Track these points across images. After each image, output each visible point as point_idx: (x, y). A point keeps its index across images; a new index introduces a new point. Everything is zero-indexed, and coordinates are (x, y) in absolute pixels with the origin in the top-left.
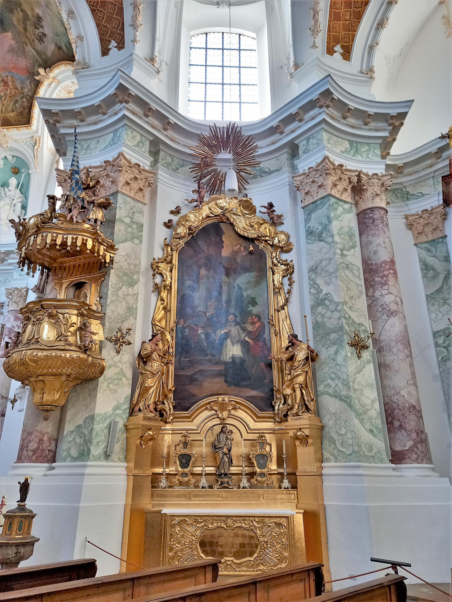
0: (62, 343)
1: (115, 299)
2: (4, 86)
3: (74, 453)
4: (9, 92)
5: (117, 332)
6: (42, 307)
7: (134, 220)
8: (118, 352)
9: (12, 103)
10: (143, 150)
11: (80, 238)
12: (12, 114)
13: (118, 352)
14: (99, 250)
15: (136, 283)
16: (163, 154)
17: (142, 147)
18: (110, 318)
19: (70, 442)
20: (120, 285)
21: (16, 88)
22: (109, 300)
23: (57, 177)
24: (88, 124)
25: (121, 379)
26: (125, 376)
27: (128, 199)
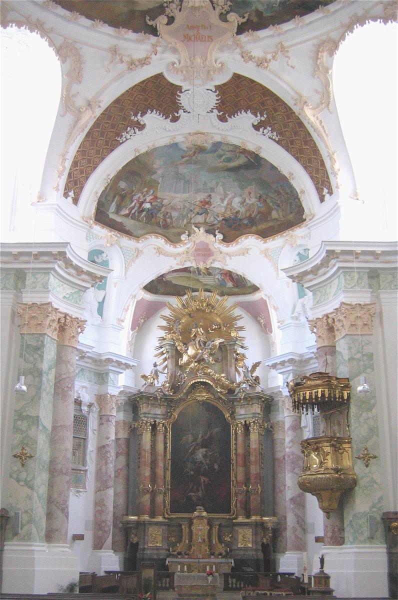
0: (322, 469)
1: (358, 425)
2: (278, 194)
3: (351, 539)
4: (283, 198)
5: (364, 451)
6: (308, 444)
7: (364, 353)
8: (367, 466)
9: (289, 206)
10: (363, 284)
11: (320, 390)
12: (291, 216)
13: (367, 466)
14: (335, 395)
15: (374, 406)
16: (383, 276)
17: (361, 283)
18: (356, 441)
19: (348, 532)
20: (361, 412)
21: (287, 194)
22: (353, 428)
23: (309, 327)
24: (320, 276)
25: (373, 486)
26: (376, 483)
27: (356, 337)
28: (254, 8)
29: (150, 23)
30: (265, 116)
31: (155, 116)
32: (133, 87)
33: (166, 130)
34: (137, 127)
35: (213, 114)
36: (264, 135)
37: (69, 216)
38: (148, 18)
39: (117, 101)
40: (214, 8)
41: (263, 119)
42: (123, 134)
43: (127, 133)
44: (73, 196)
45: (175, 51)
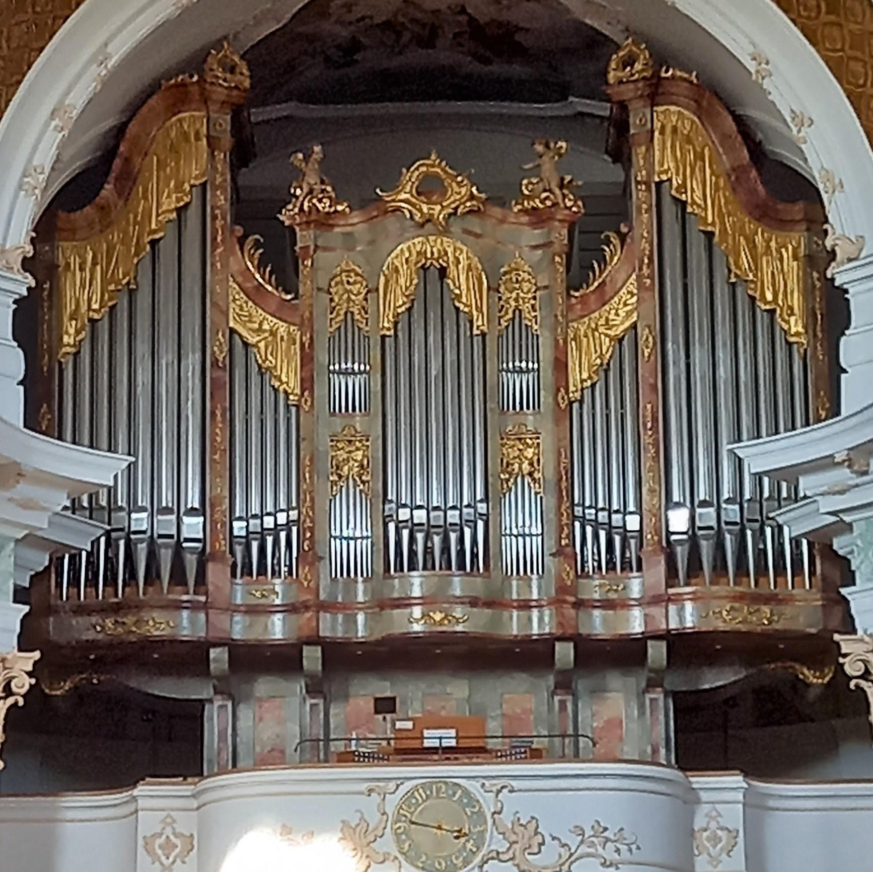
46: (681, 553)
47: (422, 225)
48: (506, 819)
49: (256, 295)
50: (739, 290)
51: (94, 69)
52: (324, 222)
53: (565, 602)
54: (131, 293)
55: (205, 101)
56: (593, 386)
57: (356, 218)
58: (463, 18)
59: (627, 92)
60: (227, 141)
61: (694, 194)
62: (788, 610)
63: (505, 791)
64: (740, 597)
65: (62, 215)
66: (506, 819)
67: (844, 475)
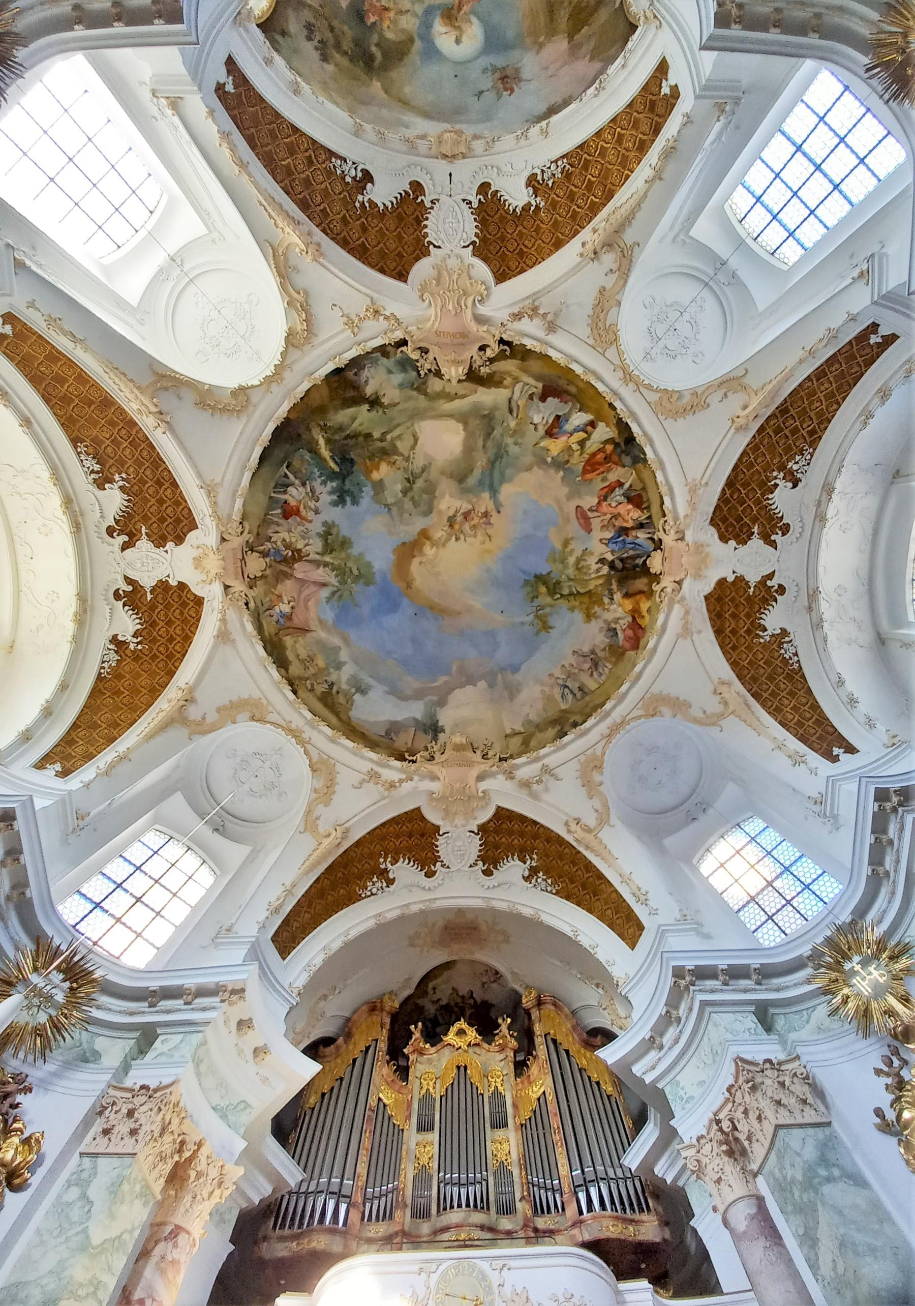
28: (392, 360)
29: (506, 347)
30: (357, 205)
31: (511, 201)
32: (534, 264)
33: (498, 169)
34: (539, 183)
35: (433, 197)
36: (354, 163)
37: (685, 55)
38: (508, 353)
39: (558, 245)
40: (435, 359)
41: (360, 198)
42: (560, 175)
43: (554, 175)
44: (664, 81)
45: (480, 320)
46: (582, 1196)
47: (458, 1049)
48: (507, 1290)
49: (390, 1084)
50: (584, 1073)
51: (343, 938)
52: (421, 1053)
53: (529, 1226)
54: (341, 1079)
55: (382, 1010)
56: (530, 1119)
57: (433, 1050)
58: (472, 1001)
59: (529, 1005)
60: (388, 1027)
61: (559, 1039)
62: (643, 1229)
63: (505, 1269)
64: (617, 1218)
65: (321, 1048)
66: (507, 1290)
67: (653, 1055)
